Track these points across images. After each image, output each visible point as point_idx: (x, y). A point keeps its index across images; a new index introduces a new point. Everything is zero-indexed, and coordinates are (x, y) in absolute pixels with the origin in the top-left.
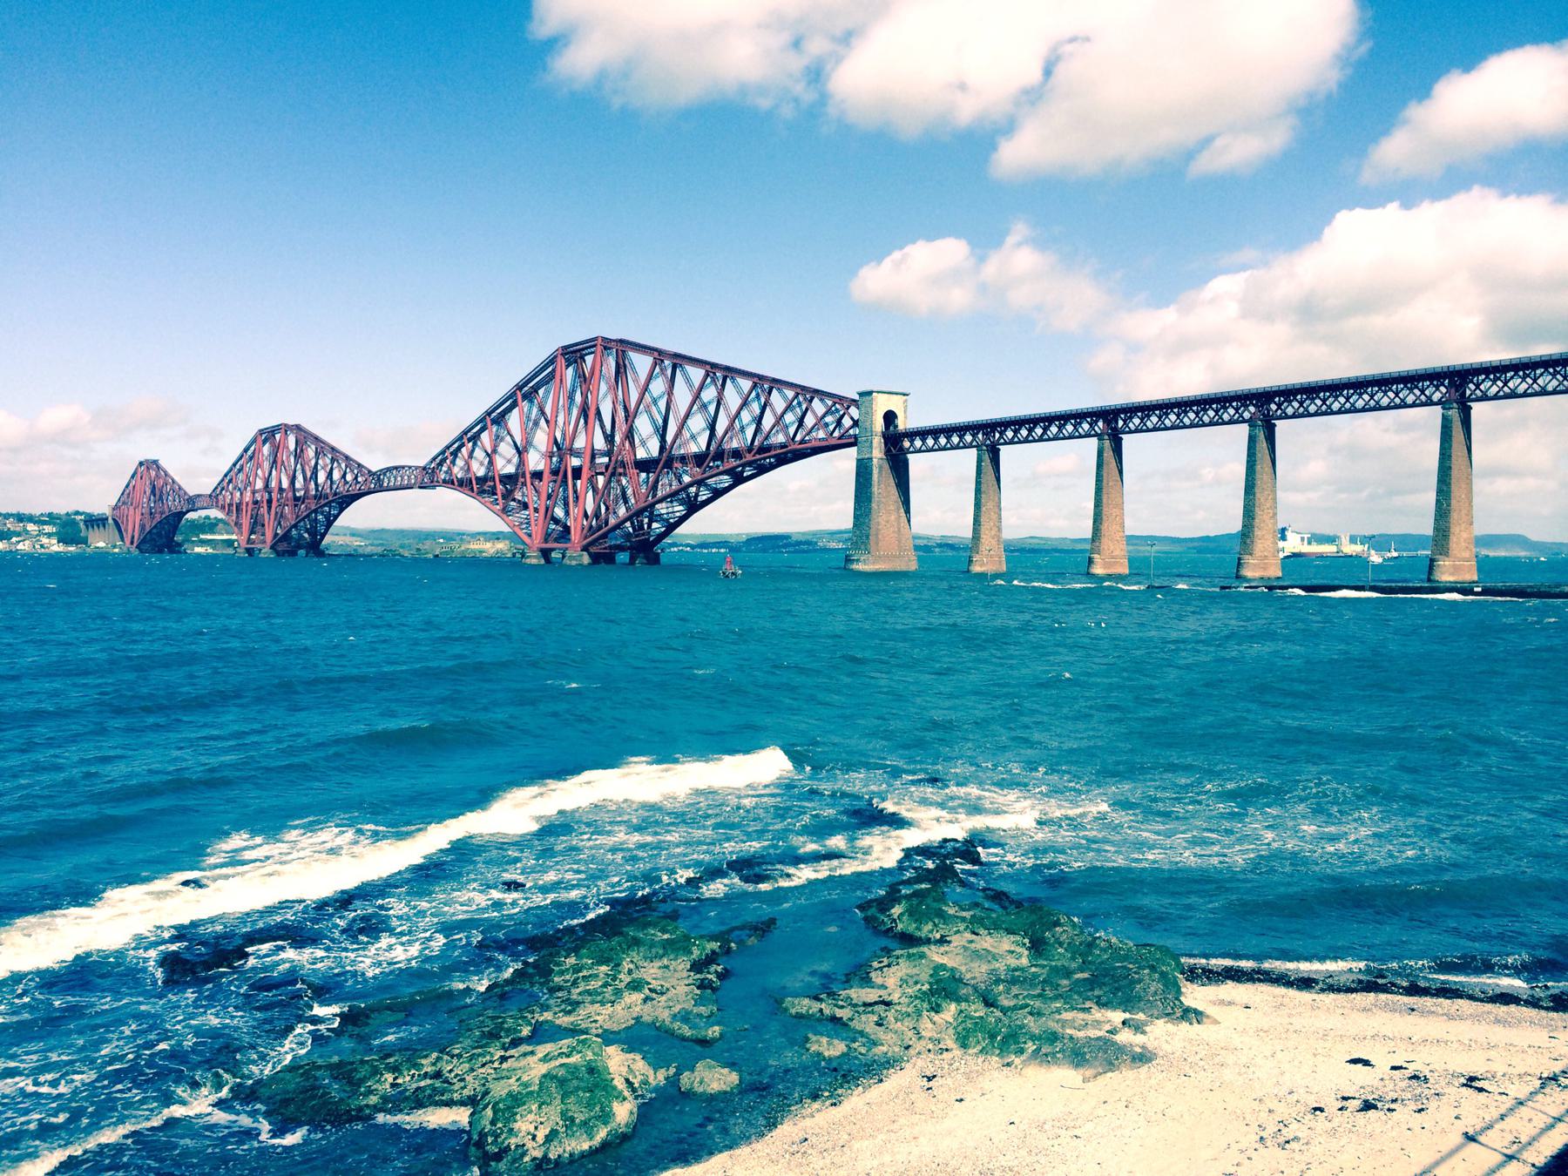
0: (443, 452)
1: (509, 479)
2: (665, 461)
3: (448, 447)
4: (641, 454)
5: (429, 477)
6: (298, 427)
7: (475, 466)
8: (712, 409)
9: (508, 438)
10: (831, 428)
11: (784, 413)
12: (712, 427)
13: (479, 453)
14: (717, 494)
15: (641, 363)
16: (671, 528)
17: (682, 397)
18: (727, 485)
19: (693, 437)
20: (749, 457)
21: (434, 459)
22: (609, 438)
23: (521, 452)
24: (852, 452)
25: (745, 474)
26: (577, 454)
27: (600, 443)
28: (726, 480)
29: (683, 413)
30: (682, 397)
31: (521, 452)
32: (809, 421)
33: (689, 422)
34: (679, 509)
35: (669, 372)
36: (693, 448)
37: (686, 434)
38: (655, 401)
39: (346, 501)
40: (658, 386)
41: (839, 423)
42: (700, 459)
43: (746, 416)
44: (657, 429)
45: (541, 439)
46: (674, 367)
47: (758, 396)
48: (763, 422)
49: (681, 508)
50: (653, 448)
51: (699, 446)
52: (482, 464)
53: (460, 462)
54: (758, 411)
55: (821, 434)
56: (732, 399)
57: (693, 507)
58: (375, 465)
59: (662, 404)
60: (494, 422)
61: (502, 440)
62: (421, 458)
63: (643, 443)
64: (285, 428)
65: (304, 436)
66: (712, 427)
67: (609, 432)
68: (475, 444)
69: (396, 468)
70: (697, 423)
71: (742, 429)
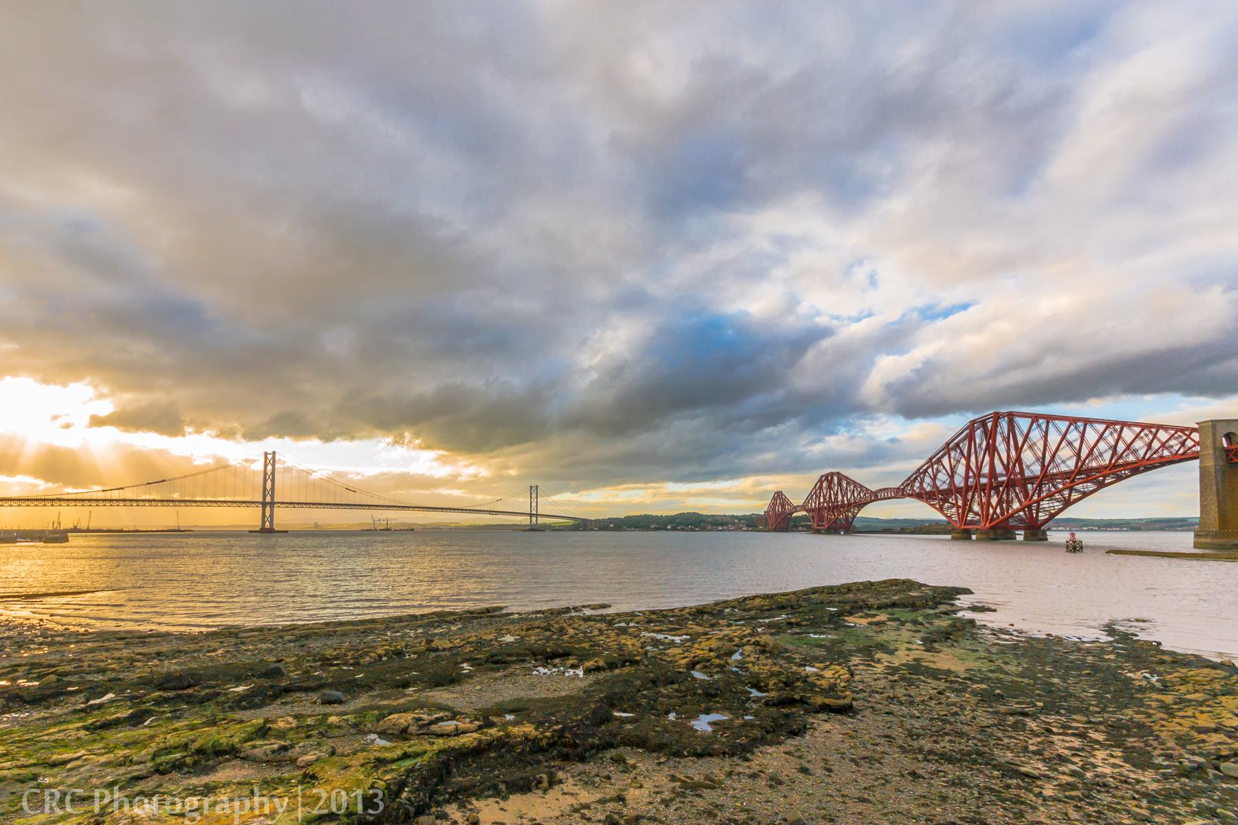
0: (907, 480)
1: (942, 492)
3: (910, 478)
4: (1027, 474)
5: (900, 493)
6: (838, 473)
7: (925, 485)
8: (1077, 444)
9: (944, 471)
11: (1133, 442)
12: (1078, 455)
13: (928, 480)
14: (1085, 495)
15: (1023, 424)
16: (1052, 516)
17: (1054, 438)
18: (1091, 489)
21: (903, 484)
22: (1006, 467)
23: (952, 477)
24: (1196, 463)
25: (1106, 482)
26: (984, 476)
27: (999, 469)
28: (1091, 486)
29: (1054, 448)
30: (1054, 438)
31: (952, 477)
32: (1156, 445)
33: (1059, 453)
34: (1058, 505)
35: (1044, 427)
36: (1063, 468)
37: (1058, 460)
38: (1035, 444)
39: (861, 505)
40: (1036, 435)
41: (1183, 444)
43: (1102, 446)
44: (1038, 459)
45: (961, 469)
46: (1048, 423)
47: (1111, 433)
48: (1118, 449)
49: (1058, 504)
50: (1037, 469)
51: (1068, 466)
52: (929, 485)
53: (917, 484)
54: (1113, 443)
55: (1166, 453)
56: (1091, 436)
57: (1067, 503)
58: (874, 487)
59: (1040, 444)
60: (935, 463)
61: (940, 471)
63: (1028, 467)
64: (832, 474)
65: (841, 477)
66: (1078, 455)
67: (1006, 463)
68: (925, 475)
69: (884, 489)
70: (1066, 452)
71: (1101, 454)
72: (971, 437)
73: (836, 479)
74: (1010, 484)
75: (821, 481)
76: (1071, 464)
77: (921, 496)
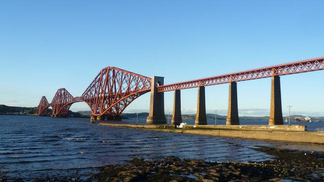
2: (120, 95)
6: (64, 89)
10: (149, 86)
14: (130, 103)
15: (116, 71)
16: (122, 111)
19: (124, 89)
20: (132, 94)
31: (96, 92)
35: (121, 74)
36: (123, 91)
37: (122, 89)
42: (123, 93)
57: (126, 106)
62: (80, 95)
71: (133, 87)
72: (102, 78)
73: (63, 92)
74: (109, 97)
75: (57, 93)
76: (126, 89)
77: (87, 101)
